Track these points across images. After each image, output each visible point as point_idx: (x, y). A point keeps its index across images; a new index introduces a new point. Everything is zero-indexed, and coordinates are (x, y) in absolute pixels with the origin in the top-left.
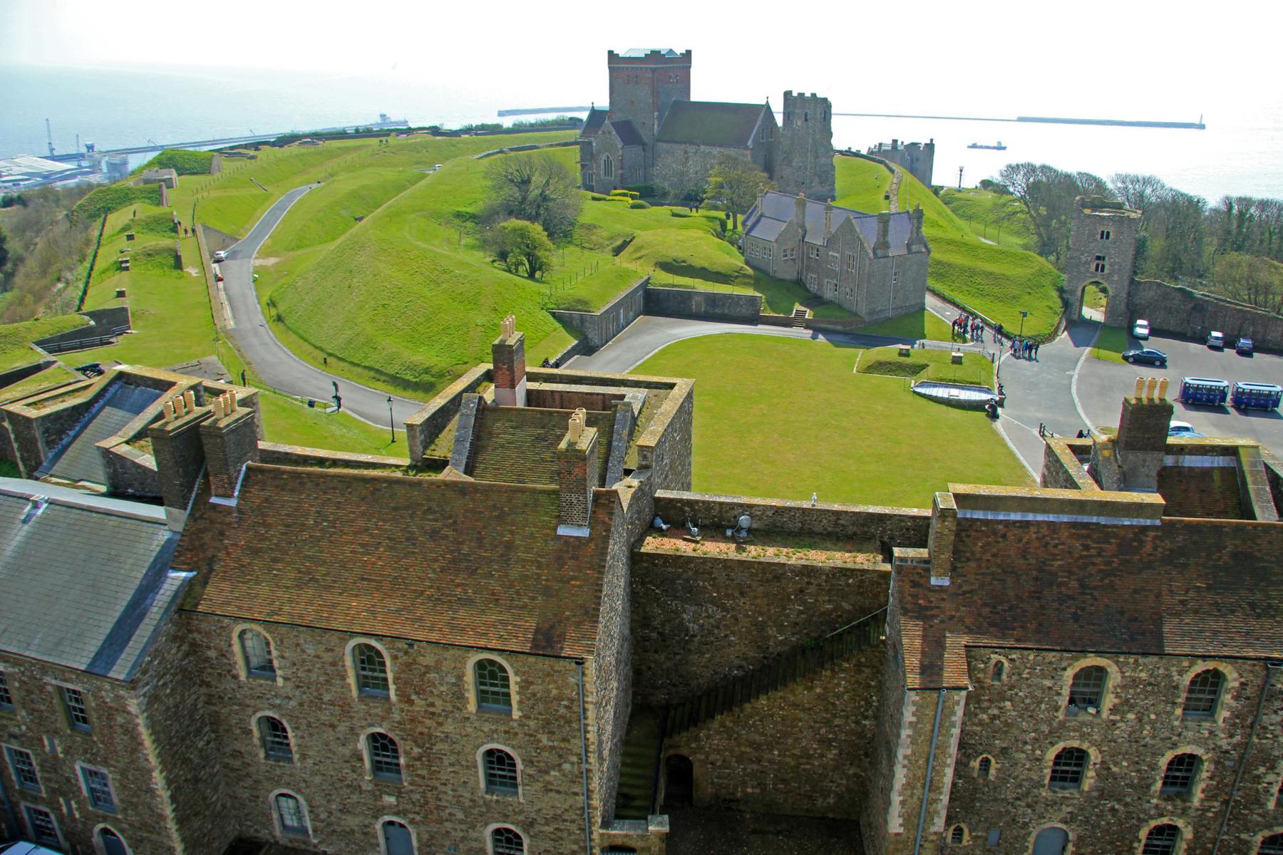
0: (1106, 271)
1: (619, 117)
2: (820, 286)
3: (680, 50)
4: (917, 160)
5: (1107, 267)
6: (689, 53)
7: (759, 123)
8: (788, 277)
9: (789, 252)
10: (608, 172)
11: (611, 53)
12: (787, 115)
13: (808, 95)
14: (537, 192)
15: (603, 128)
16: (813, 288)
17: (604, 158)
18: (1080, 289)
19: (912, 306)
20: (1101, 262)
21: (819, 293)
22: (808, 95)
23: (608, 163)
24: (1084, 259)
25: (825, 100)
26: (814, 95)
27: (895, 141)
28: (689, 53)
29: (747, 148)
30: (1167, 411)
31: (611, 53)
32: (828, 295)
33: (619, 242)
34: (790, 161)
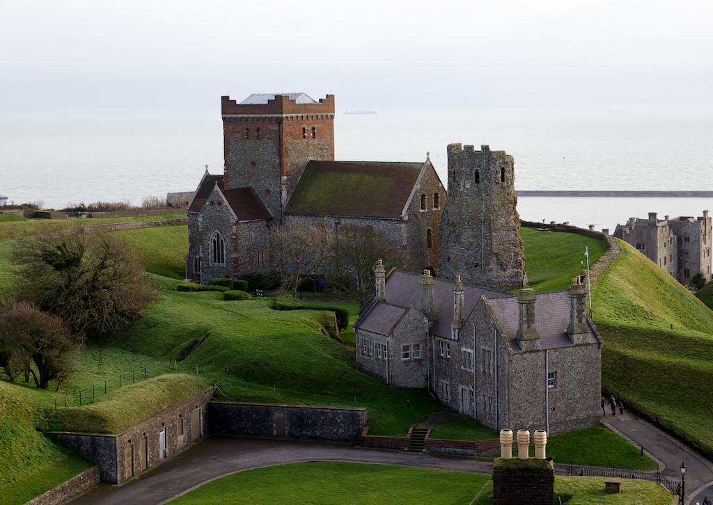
1: (234, 184)
3: (316, 95)
4: (687, 240)
6: (330, 98)
7: (417, 187)
8: (411, 384)
9: (411, 350)
10: (218, 256)
11: (225, 99)
12: (452, 175)
13: (478, 148)
14: (87, 276)
15: (212, 197)
16: (446, 397)
17: (212, 236)
19: (582, 421)
21: (453, 405)
22: (478, 148)
23: (218, 245)
25: (501, 155)
26: (486, 148)
27: (652, 215)
28: (330, 98)
29: (401, 221)
30: (548, 478)
31: (225, 99)
32: (465, 406)
33: (185, 344)
34: (458, 237)
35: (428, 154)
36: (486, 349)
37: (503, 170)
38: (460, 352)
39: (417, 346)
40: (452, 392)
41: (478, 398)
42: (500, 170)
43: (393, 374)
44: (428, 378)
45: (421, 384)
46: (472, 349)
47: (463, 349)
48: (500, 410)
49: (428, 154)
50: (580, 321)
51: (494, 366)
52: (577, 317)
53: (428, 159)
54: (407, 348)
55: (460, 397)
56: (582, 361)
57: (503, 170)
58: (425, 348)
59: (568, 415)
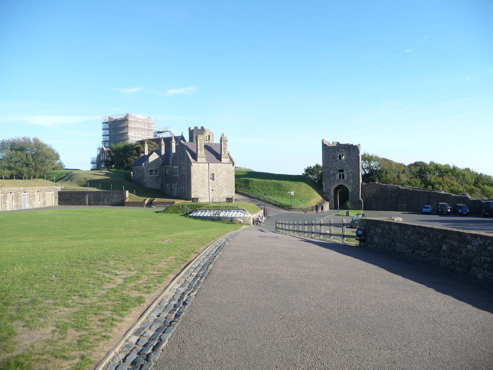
0: (345, 178)
2: (171, 189)
5: (345, 175)
13: (199, 128)
18: (332, 190)
20: (342, 173)
22: (199, 128)
24: (332, 173)
35: (182, 132)
36: (183, 164)
37: (209, 136)
38: (173, 169)
39: (156, 171)
40: (170, 188)
41: (180, 187)
42: (208, 136)
43: (145, 181)
44: (162, 185)
45: (158, 186)
46: (177, 166)
47: (175, 167)
48: (188, 190)
49: (182, 132)
50: (225, 153)
51: (185, 170)
52: (223, 151)
53: (182, 134)
54: (151, 171)
55: (173, 189)
56: (226, 170)
57: (209, 136)
58: (160, 172)
59: (220, 194)
